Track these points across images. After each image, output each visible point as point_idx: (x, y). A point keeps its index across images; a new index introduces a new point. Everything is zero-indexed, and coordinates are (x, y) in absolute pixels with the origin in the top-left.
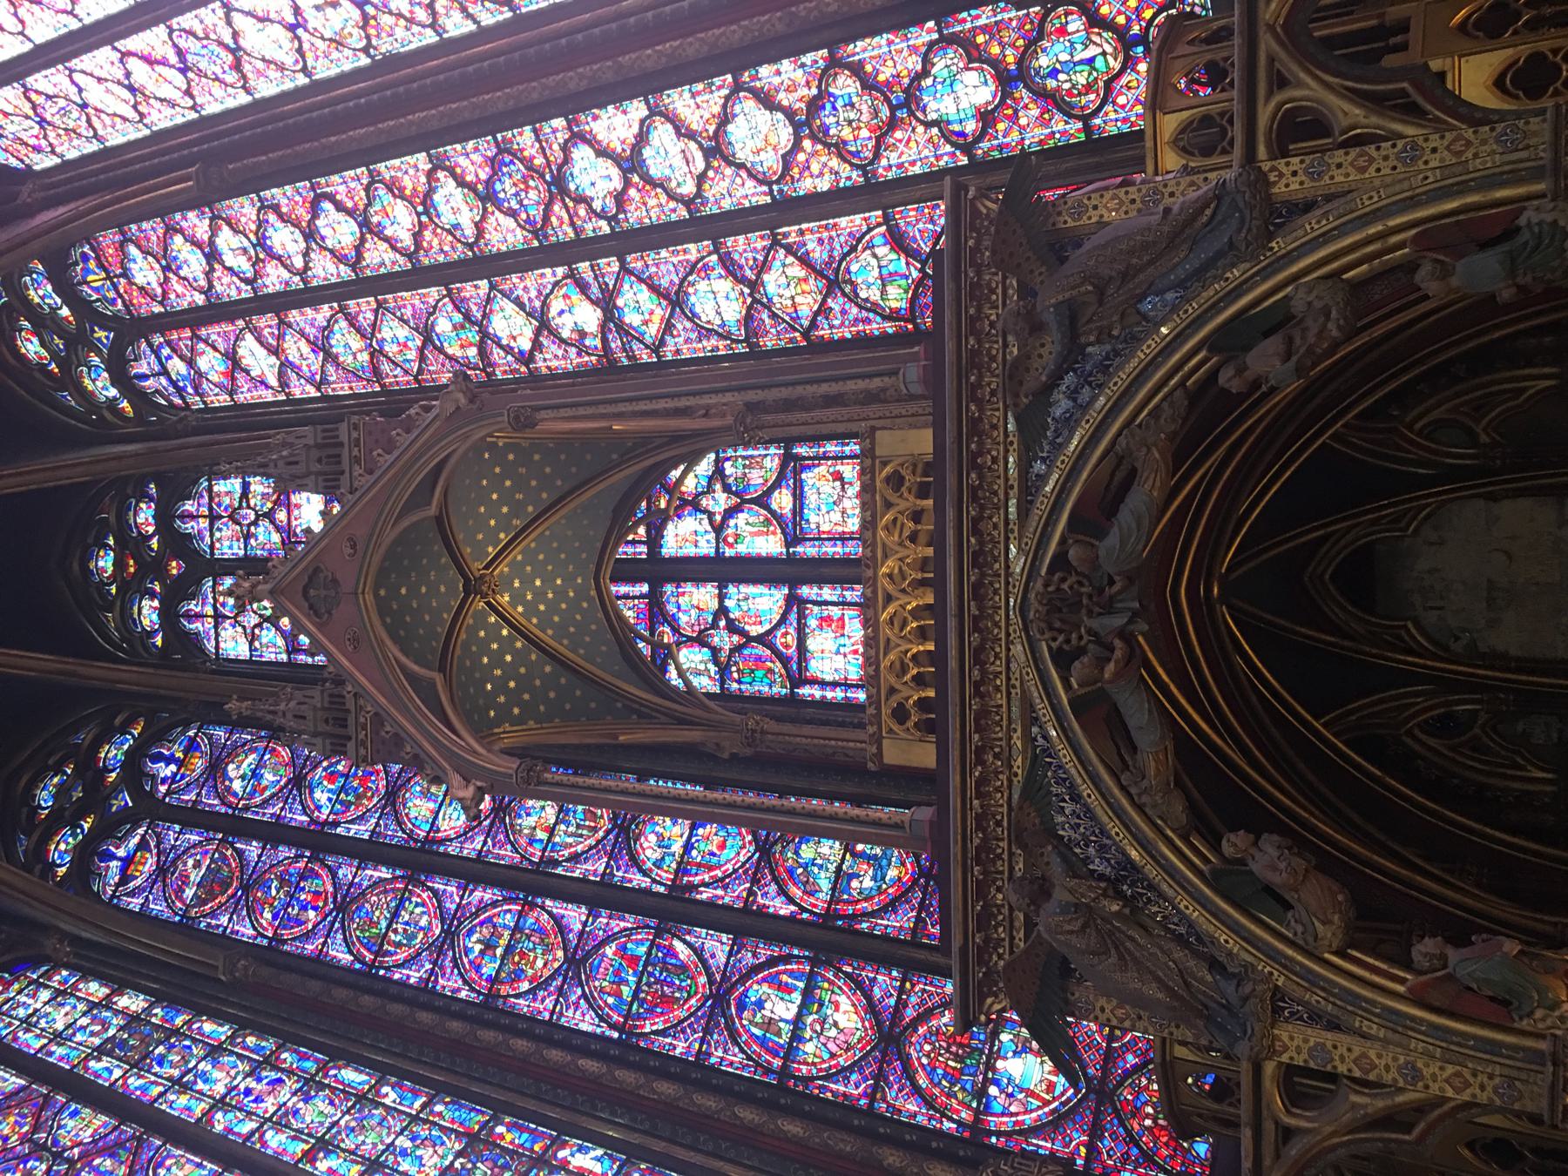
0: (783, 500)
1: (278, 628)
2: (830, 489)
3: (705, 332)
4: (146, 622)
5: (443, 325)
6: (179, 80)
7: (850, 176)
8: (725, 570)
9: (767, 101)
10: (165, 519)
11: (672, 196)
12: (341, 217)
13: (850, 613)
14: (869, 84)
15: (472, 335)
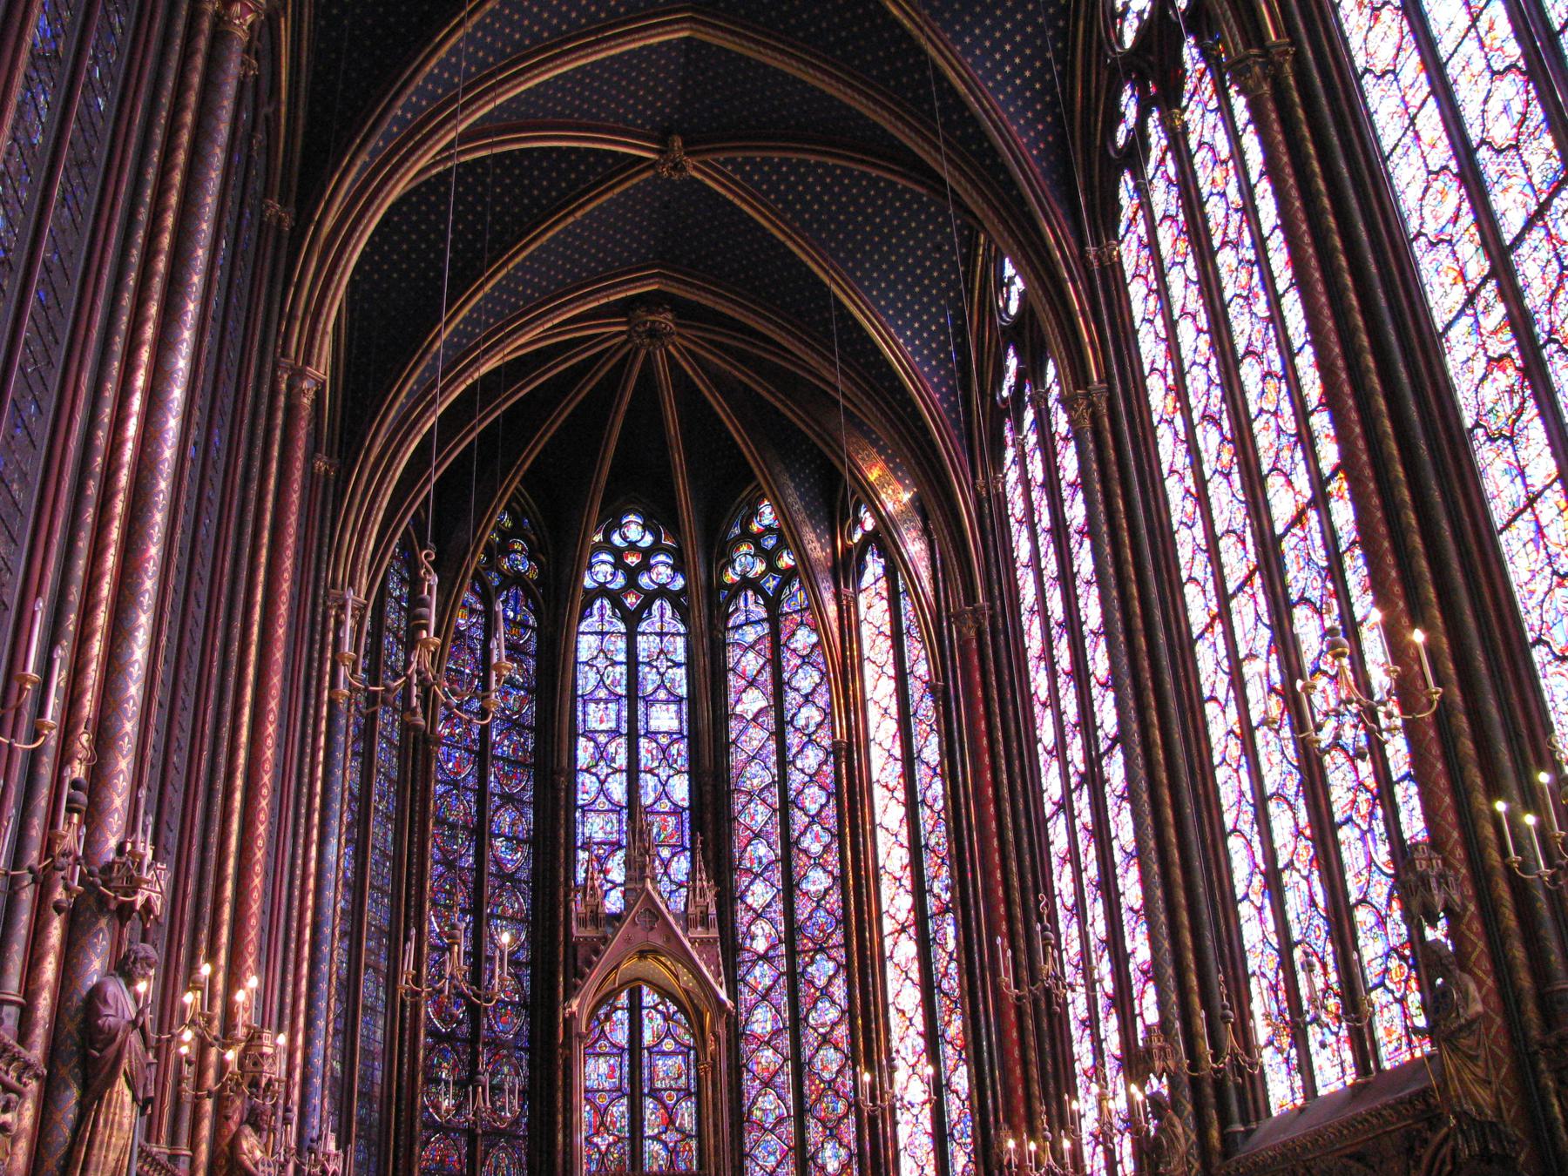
0: (669, 1045)
1: (597, 687)
2: (674, 1072)
3: (750, 1011)
4: (597, 568)
5: (761, 850)
6: (887, 744)
7: (808, 1103)
8: (635, 1009)
9: (839, 1072)
10: (662, 591)
11: (809, 1011)
12: (817, 806)
13: (616, 1081)
14: (840, 1119)
15: (756, 869)
